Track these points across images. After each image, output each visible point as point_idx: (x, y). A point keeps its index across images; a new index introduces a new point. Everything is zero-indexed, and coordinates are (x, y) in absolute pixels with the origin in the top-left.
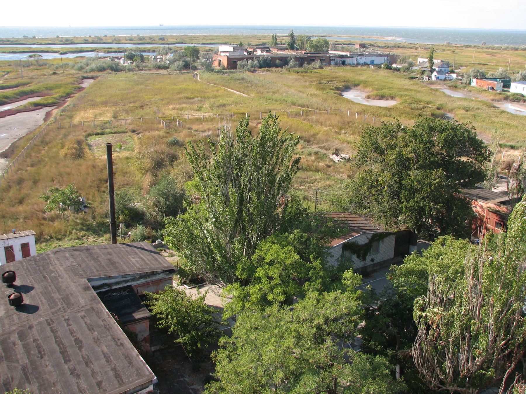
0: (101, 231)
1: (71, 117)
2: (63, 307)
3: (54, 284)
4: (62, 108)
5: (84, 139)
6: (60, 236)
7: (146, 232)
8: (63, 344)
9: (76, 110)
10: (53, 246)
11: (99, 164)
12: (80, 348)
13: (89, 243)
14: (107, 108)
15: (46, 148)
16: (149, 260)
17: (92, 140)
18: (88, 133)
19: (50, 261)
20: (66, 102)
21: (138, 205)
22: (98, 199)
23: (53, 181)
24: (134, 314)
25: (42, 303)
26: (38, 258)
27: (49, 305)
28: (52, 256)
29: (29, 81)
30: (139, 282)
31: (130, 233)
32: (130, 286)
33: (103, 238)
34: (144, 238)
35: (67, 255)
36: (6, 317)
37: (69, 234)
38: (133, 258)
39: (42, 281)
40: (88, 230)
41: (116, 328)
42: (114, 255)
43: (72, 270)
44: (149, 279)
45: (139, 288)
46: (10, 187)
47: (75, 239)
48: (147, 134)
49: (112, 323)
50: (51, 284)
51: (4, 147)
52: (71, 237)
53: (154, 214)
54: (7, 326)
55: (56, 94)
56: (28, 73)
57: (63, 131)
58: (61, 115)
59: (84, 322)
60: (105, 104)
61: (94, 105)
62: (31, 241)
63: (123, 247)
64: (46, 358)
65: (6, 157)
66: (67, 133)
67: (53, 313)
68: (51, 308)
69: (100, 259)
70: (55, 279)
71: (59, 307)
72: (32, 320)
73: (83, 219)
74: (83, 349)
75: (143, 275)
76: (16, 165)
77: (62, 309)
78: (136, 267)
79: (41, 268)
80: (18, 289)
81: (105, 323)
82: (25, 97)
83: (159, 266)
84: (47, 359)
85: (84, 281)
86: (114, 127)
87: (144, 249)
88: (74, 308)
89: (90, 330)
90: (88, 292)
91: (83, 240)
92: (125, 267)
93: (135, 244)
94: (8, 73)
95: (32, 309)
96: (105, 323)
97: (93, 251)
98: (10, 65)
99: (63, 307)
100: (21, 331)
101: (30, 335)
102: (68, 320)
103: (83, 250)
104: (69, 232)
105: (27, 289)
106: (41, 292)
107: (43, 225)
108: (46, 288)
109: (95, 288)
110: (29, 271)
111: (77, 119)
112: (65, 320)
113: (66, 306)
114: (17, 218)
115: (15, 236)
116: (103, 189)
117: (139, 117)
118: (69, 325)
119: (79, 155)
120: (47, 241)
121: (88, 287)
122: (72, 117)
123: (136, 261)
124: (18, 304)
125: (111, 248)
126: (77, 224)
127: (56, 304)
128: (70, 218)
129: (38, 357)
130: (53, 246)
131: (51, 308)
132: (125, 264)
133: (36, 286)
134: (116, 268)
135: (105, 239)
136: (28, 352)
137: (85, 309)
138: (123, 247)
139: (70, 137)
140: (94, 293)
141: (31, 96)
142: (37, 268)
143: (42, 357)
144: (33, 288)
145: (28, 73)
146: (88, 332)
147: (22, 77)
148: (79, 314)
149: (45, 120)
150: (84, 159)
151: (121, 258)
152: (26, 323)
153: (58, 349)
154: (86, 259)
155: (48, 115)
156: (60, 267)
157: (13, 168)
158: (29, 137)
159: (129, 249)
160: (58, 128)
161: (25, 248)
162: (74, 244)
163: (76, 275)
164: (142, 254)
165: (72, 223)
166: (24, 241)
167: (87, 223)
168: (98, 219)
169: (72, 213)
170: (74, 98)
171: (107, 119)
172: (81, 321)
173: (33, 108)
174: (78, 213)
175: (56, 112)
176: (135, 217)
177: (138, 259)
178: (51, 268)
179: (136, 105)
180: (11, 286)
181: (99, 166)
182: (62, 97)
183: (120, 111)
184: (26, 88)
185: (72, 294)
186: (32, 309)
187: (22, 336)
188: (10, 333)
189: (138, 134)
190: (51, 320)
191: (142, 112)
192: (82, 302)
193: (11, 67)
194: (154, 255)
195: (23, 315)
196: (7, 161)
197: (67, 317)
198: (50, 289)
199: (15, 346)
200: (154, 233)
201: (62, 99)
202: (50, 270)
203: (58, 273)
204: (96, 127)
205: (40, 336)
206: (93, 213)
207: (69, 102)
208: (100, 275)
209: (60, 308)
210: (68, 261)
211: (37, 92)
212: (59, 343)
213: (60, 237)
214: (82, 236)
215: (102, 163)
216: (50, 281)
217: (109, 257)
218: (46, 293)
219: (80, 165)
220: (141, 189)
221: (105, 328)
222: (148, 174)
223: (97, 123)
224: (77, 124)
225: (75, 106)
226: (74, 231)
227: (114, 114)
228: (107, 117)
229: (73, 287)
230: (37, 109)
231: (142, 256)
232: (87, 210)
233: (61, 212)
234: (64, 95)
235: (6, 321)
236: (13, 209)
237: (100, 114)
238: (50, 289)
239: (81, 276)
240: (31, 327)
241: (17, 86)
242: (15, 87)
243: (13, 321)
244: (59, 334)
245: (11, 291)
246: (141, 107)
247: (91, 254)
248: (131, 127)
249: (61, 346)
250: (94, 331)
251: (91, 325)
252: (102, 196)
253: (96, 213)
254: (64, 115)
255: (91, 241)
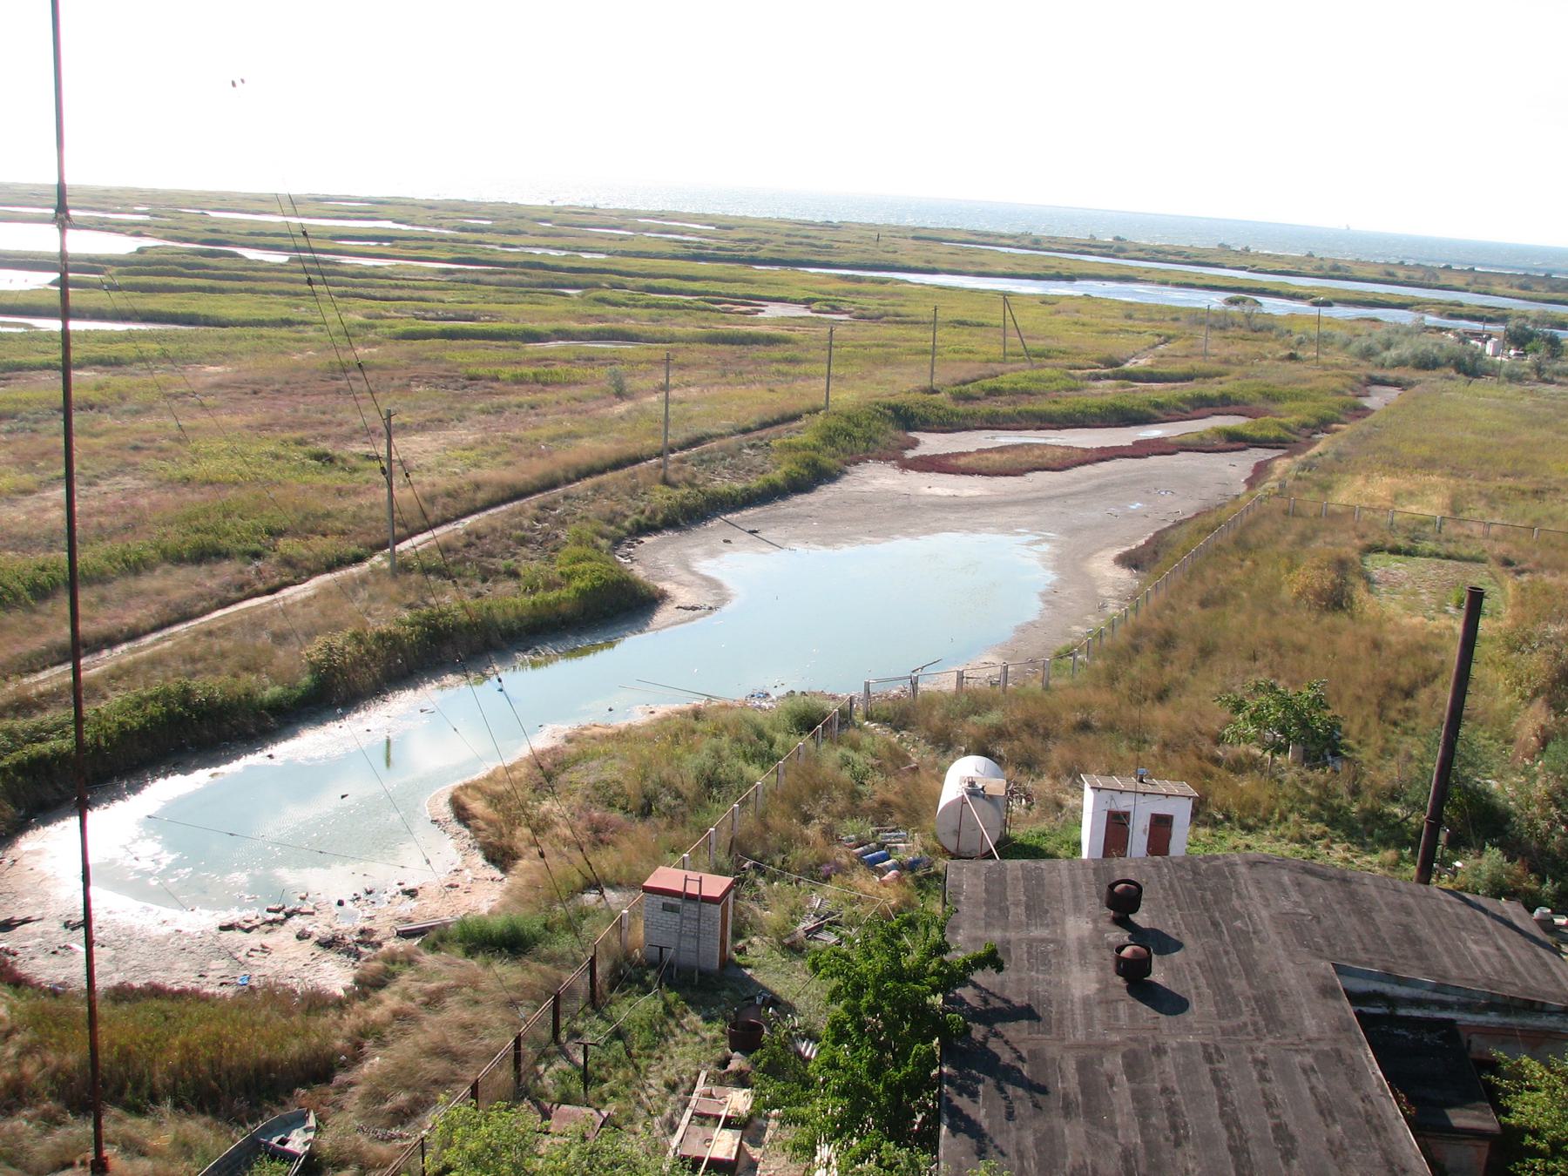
0: (1371, 834)
1: (1325, 488)
2: (1255, 1024)
3: (1238, 951)
4: (1300, 458)
5: (1355, 555)
6: (1252, 820)
7: (1509, 874)
8: (1239, 1127)
9: (1342, 472)
10: (1230, 842)
11: (1392, 638)
12: (1288, 1155)
13: (1331, 861)
14: (1434, 479)
15: (1248, 563)
16: (1522, 963)
17: (1378, 565)
18: (1368, 541)
19: (1237, 883)
20: (1315, 443)
21: (1501, 787)
22: (1376, 741)
23: (1254, 658)
24: (1449, 1112)
25: (1199, 995)
26: (1204, 866)
27: (1216, 1004)
28: (1242, 869)
29: (1222, 368)
30: (1480, 1019)
31: (1458, 864)
32: (1452, 1021)
33: (1375, 859)
34: (1499, 890)
35: (1286, 879)
36: (1100, 1003)
37: (1280, 822)
38: (1476, 942)
39: (1206, 933)
40: (1332, 823)
41: (1401, 1133)
42: (1419, 917)
43: (1293, 925)
44: (1513, 1020)
45: (1474, 1038)
46: (1136, 649)
47: (1291, 840)
48: (1548, 579)
49: (1391, 1116)
50: (1230, 948)
51: (1133, 539)
52: (1281, 829)
53: (1543, 825)
54: (1098, 1028)
55: (1292, 415)
56: (1218, 347)
57: (1298, 525)
58: (1299, 478)
59: (1307, 1085)
60: (1428, 464)
61: (1395, 464)
62: (1181, 812)
63: (1449, 902)
64: (1189, 1148)
65: (1136, 567)
66: (1309, 532)
67: (1224, 1032)
68: (1220, 1016)
69: (1378, 919)
70: (1241, 937)
71: (1243, 1018)
72: (1166, 1031)
73: (1324, 788)
74: (1295, 1163)
75: (1499, 1000)
76: (1162, 593)
77: (1250, 1028)
78: (1483, 971)
79: (1209, 895)
80: (1138, 934)
81: (1369, 1107)
82: (1205, 411)
83: (1552, 988)
84: (1192, 1153)
85: (1325, 967)
86: (1448, 541)
87: (1510, 925)
88: (1284, 1036)
89: (1321, 1113)
90: (1331, 1002)
91: (1314, 847)
92: (1447, 960)
93: (1486, 902)
94: (1168, 339)
95: (1169, 1003)
96: (1369, 1107)
97: (1361, 890)
98: (1176, 320)
99: (1255, 1024)
100: (1133, 1051)
101: (1156, 1070)
102: (1264, 1064)
103: (1331, 878)
104: (1281, 814)
105: (1166, 944)
106: (1199, 964)
107: (1210, 776)
108: (1215, 955)
109: (1354, 998)
110: (1175, 895)
111: (1345, 495)
112: (1256, 1061)
113: (1262, 1023)
114: (1145, 741)
115: (1141, 788)
116: (1393, 714)
117: (1527, 522)
118: (1263, 1078)
119: (1336, 601)
120: (1216, 824)
121: (1335, 989)
122: (1329, 487)
123: (1484, 954)
124: (1134, 974)
125: (1413, 895)
126: (1306, 799)
127: (1237, 1011)
128: (1290, 776)
129: (1167, 1139)
130: (1230, 842)
131: (1220, 1016)
132: (1448, 950)
133: (1188, 940)
134: (1421, 957)
135: (1373, 863)
136: (1143, 1113)
137: (1316, 1048)
138: (1449, 902)
139: (1317, 544)
140: (1350, 1011)
141: (1221, 410)
142: (1199, 894)
143: (1177, 1144)
144: (1178, 946)
145: (1218, 347)
146: (1315, 1117)
147: (1206, 354)
148: (1298, 1058)
149: (1251, 483)
150: (1352, 617)
151: (1437, 933)
152: (1147, 1035)
153: (1224, 1135)
154: (1336, 907)
155: (1261, 470)
156: (1260, 909)
157: (1152, 599)
158: (1204, 522)
159: (1465, 911)
160: (1286, 513)
161: (1161, 826)
162: (1286, 853)
163: (1302, 945)
164: (1503, 937)
165: (1291, 792)
166: (1162, 808)
167: (1336, 802)
168: (1369, 801)
169: (1294, 762)
170: (1338, 434)
171: (1427, 512)
172: (1300, 1077)
173: (1221, 444)
174: (1311, 769)
175: (1283, 465)
176: (1485, 822)
177: (1490, 950)
178: (1236, 903)
179: (1523, 487)
180: (1122, 921)
181: (1389, 644)
182: (1305, 426)
183: (1470, 493)
184: (1212, 389)
185: (1284, 995)
186: (1169, 1003)
187: (1134, 1065)
188: (1106, 1047)
189: (1519, 573)
190: (1217, 1049)
191: (1537, 509)
192: (1310, 1025)
193: (1177, 324)
194: (1541, 951)
195: (1144, 1010)
196: (1137, 577)
197: (1261, 1056)
198: (1225, 960)
199: (1111, 1086)
200: (1531, 883)
201: (1306, 432)
202: (1233, 909)
203: (1254, 925)
204: (1393, 528)
205: (1179, 1081)
206: (1355, 778)
207: (1323, 444)
208: (1371, 965)
209: (1245, 1024)
210: (1287, 898)
211: (1237, 403)
212: (1231, 1122)
213: (1251, 822)
214: (1314, 837)
215: (1402, 638)
216: (1227, 938)
217: (1404, 919)
218: (1214, 971)
219: (1333, 630)
220: (1509, 741)
221: (1368, 1122)
222: (1539, 701)
223: (1397, 518)
224: (1339, 510)
225: (1339, 456)
226: (1294, 817)
227: (1453, 503)
228: (1431, 505)
229: (1290, 976)
230: (1233, 450)
231: (1502, 943)
232: (1339, 765)
233: (1268, 755)
234: (1313, 421)
235: (1098, 1013)
236: (1135, 713)
237: (1411, 494)
238: (1225, 960)
239: (1318, 952)
240: (1159, 1051)
241: (1187, 377)
242: (1181, 380)
243: (1117, 1018)
244: (1233, 1093)
245: (1118, 935)
246: (1538, 493)
247: (1352, 896)
248: (1500, 549)
249: (1235, 1130)
250: (1334, 1121)
251: (1327, 1100)
252: (1389, 735)
253: (1365, 781)
254: (1306, 479)
255: (1337, 854)
